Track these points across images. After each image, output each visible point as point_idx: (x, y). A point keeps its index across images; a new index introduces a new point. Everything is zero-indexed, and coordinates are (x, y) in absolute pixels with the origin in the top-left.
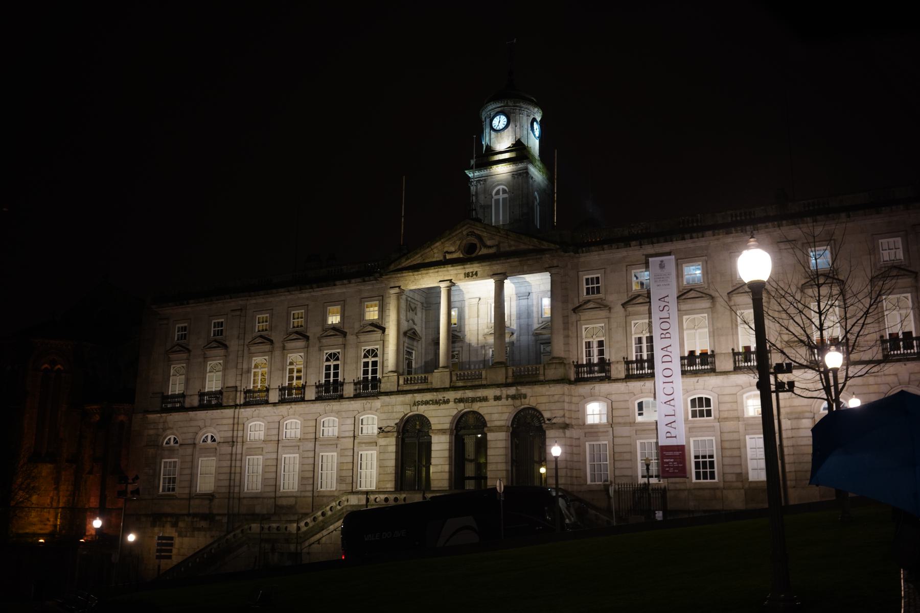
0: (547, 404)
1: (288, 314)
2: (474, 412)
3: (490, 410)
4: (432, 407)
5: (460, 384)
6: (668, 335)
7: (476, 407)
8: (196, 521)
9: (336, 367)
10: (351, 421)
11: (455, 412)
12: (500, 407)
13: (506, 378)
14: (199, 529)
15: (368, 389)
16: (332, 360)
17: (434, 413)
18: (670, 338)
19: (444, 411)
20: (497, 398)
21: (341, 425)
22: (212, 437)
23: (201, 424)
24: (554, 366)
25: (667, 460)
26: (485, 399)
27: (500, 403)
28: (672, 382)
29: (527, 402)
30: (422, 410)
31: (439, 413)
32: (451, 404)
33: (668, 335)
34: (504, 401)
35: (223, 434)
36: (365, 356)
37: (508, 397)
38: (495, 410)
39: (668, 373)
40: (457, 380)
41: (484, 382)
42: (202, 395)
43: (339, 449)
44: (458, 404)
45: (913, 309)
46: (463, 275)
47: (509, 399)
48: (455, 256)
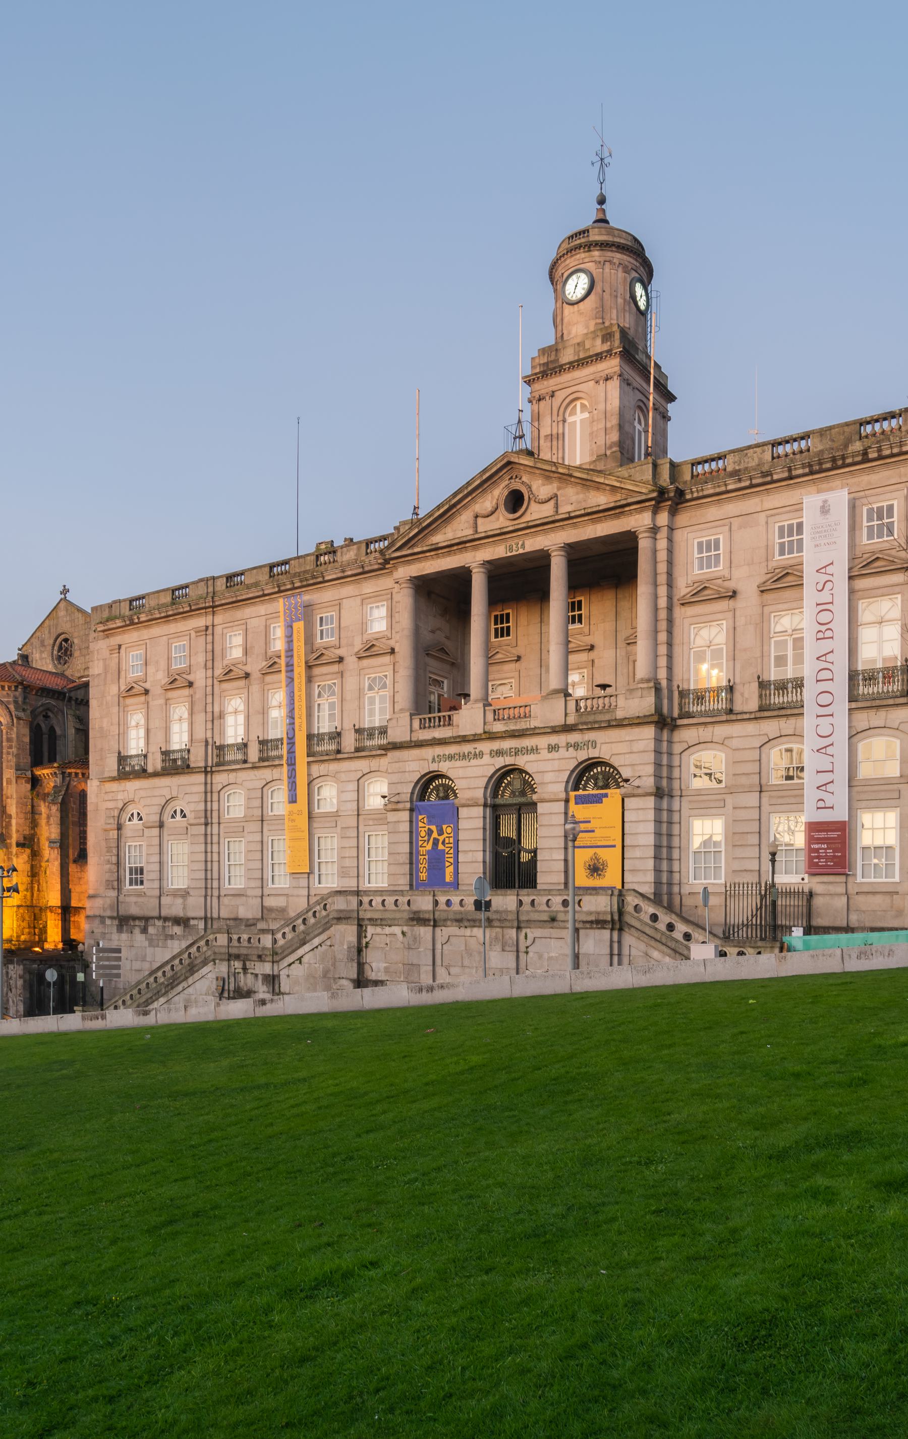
0: (627, 756)
1: (267, 628)
2: (521, 771)
3: (542, 766)
4: (459, 763)
5: (499, 727)
6: (828, 634)
7: (521, 761)
10: (353, 787)
12: (556, 762)
13: (566, 715)
17: (461, 773)
18: (832, 638)
19: (475, 768)
20: (552, 748)
21: (340, 792)
22: (182, 811)
24: (639, 693)
25: (816, 846)
26: (535, 750)
27: (554, 755)
28: (832, 715)
30: (444, 767)
31: (470, 772)
32: (486, 759)
34: (562, 752)
35: (193, 807)
36: (371, 688)
37: (568, 746)
38: (548, 766)
39: (825, 699)
40: (495, 720)
41: (534, 723)
42: (166, 753)
43: (339, 828)
44: (496, 759)
47: (571, 749)
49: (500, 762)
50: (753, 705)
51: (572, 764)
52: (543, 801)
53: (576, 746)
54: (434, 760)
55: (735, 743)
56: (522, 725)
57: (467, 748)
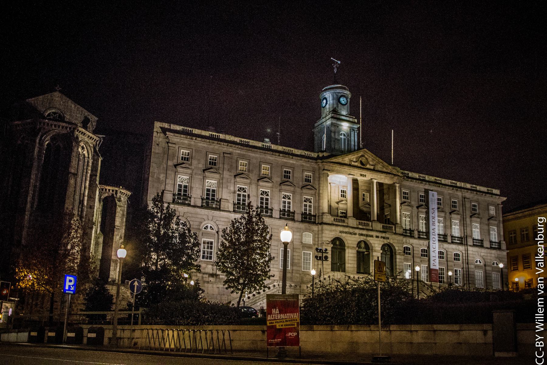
4: (349, 235)
5: (360, 227)
8: (206, 277)
9: (289, 203)
11: (359, 240)
14: (208, 282)
15: (307, 219)
16: (265, 195)
17: (349, 238)
20: (377, 237)
23: (205, 217)
26: (372, 236)
29: (389, 241)
32: (357, 236)
33: (434, 224)
34: (380, 238)
37: (381, 237)
38: (376, 242)
41: (371, 228)
45: (497, 232)
46: (359, 175)
48: (356, 164)
49: (362, 238)
50: (417, 236)
51: (383, 244)
52: (375, 251)
53: (384, 238)
54: (340, 232)
55: (414, 245)
56: (368, 228)
57: (351, 230)
